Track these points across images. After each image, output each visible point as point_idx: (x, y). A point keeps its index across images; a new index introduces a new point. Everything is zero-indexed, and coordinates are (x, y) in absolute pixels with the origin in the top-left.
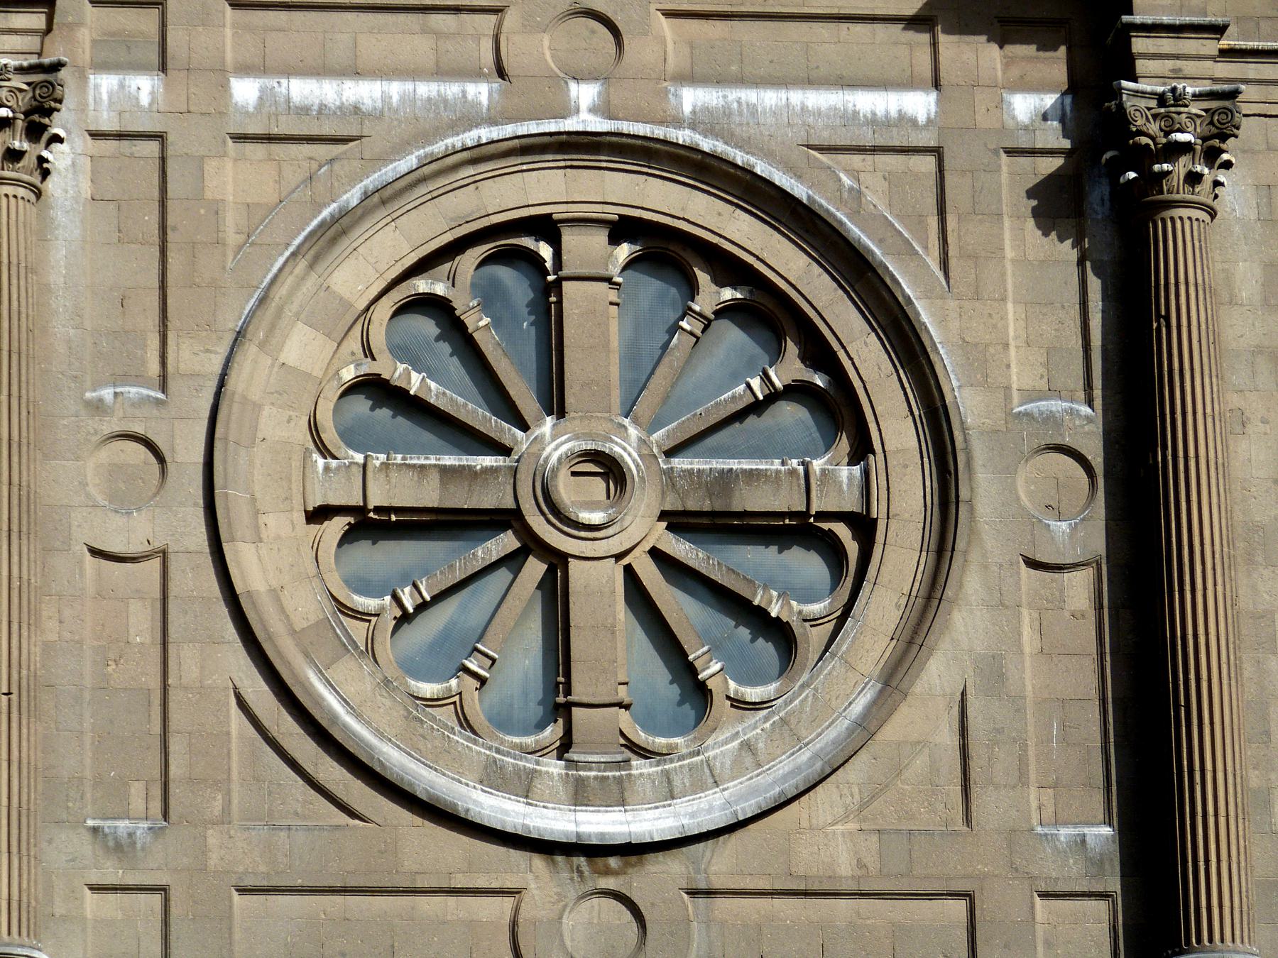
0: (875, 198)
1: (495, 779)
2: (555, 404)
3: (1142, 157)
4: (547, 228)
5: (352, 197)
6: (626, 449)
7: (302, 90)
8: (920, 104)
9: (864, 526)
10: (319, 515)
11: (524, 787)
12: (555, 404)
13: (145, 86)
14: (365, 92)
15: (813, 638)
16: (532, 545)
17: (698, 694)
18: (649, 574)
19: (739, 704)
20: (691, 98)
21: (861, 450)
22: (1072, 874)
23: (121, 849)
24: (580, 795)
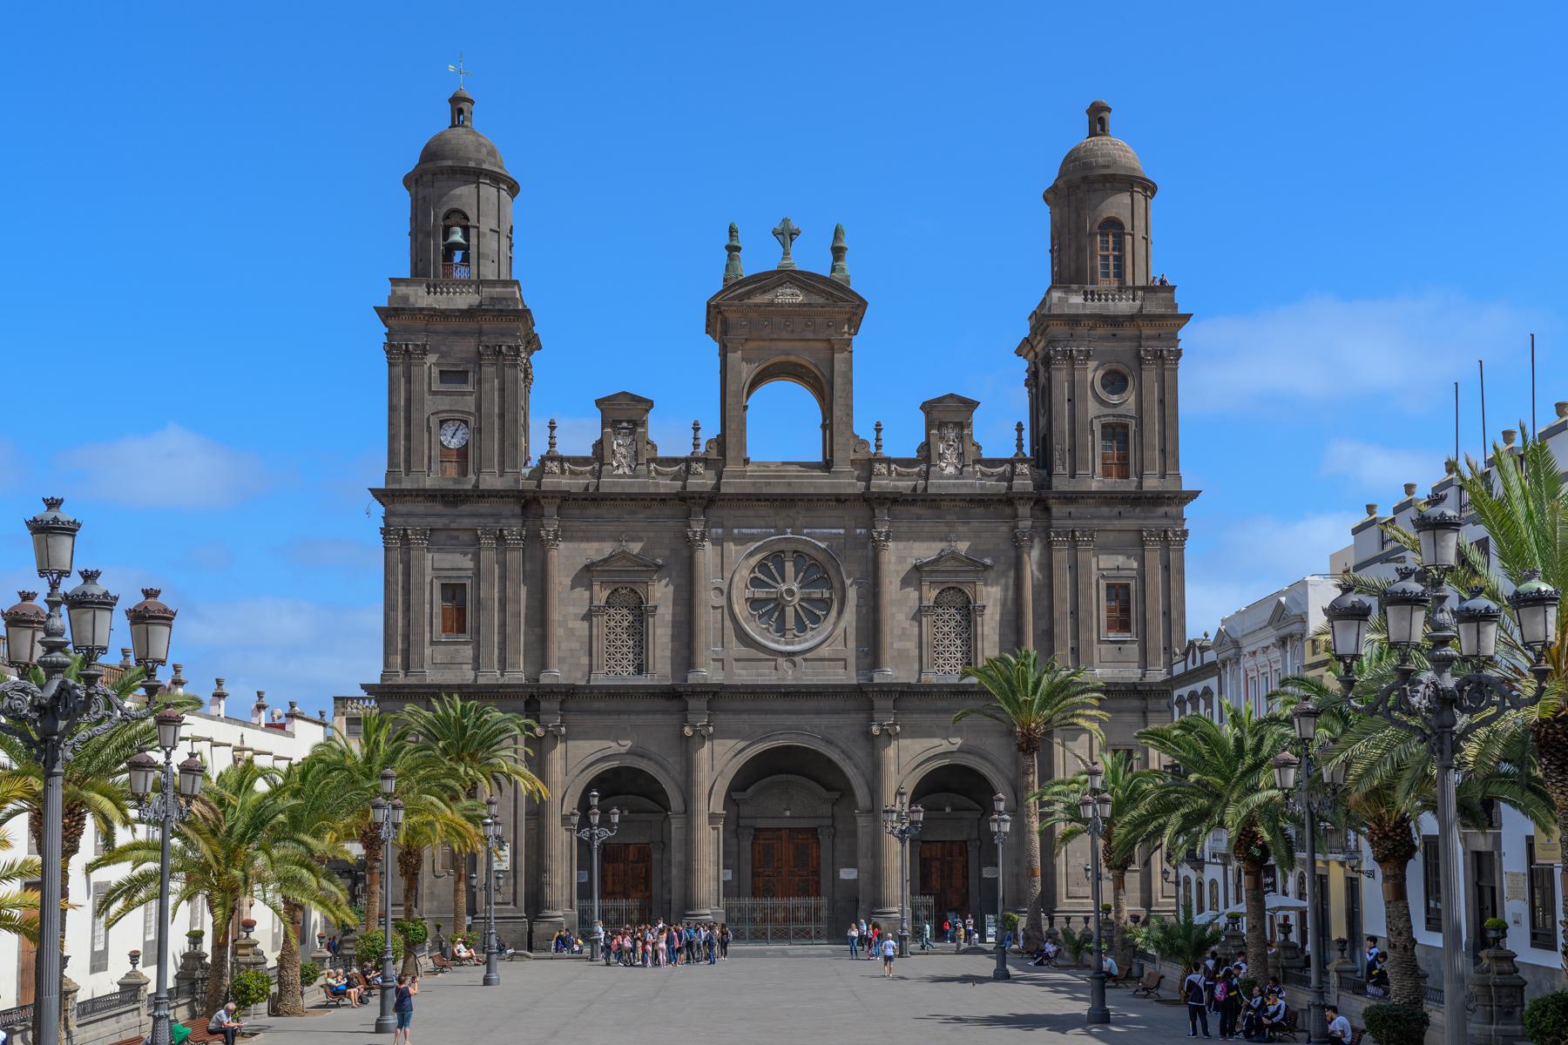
2: (784, 581)
3: (874, 541)
4: (783, 552)
6: (794, 588)
7: (744, 531)
8: (842, 531)
10: (747, 600)
11: (777, 642)
12: (784, 581)
13: (720, 531)
14: (754, 531)
15: (822, 618)
18: (797, 606)
20: (805, 531)
23: (717, 652)
24: (787, 644)
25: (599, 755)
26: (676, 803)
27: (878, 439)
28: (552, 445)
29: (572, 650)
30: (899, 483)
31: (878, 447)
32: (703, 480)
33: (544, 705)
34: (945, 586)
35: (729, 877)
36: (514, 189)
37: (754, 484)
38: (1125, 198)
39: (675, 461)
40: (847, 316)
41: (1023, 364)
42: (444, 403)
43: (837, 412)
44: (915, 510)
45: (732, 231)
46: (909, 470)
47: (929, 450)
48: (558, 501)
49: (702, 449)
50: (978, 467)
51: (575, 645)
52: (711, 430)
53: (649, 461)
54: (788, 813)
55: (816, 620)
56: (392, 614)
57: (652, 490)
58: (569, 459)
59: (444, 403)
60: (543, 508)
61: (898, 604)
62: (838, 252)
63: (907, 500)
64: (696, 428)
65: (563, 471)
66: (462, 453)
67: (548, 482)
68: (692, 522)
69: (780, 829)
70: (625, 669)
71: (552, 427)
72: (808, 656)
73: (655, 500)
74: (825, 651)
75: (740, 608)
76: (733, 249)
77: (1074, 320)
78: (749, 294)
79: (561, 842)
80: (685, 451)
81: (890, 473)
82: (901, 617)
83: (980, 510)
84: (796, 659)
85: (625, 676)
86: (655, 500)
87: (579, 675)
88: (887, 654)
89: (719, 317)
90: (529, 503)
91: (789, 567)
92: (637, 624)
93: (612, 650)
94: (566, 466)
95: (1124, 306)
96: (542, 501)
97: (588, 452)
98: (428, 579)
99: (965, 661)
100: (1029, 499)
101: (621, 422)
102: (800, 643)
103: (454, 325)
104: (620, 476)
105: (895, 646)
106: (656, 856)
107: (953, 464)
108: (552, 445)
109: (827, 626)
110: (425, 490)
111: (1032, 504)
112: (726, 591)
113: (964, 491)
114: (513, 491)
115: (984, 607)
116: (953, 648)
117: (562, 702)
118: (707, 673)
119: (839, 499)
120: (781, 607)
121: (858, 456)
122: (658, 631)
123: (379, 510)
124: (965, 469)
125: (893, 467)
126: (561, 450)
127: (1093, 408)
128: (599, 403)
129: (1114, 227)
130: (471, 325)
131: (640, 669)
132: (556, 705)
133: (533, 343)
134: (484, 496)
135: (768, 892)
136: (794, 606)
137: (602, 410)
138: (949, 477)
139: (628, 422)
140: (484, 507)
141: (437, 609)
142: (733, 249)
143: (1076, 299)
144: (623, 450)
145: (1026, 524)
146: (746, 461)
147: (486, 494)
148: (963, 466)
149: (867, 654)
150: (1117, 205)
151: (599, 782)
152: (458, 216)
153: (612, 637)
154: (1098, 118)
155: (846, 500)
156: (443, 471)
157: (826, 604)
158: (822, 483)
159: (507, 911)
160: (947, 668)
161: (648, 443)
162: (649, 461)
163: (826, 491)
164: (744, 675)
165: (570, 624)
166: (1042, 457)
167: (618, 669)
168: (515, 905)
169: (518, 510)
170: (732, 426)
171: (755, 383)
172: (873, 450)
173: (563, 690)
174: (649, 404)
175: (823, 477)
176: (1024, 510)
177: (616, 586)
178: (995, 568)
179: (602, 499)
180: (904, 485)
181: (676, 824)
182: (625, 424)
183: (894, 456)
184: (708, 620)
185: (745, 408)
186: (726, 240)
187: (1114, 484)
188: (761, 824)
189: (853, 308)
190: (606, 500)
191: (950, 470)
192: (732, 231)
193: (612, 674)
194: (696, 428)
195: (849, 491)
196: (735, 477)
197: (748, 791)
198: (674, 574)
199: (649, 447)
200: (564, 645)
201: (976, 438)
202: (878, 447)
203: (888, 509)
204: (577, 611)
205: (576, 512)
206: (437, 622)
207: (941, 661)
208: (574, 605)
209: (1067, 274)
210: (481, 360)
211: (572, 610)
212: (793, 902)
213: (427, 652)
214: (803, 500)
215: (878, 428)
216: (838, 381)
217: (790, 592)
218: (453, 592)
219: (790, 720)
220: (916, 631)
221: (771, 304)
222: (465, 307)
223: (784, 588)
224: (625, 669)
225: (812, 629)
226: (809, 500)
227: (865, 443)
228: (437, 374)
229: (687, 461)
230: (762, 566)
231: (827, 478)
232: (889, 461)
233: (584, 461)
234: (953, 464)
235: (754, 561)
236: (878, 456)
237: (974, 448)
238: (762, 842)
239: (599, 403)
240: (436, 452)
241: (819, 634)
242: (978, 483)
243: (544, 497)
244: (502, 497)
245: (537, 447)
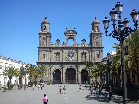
26: (61, 72)
32: (64, 46)
36: (49, 24)
38: (97, 24)
41: (90, 37)
52: (65, 42)
61: (80, 55)
67: (52, 47)
75: (67, 56)
77: (94, 34)
79: (52, 76)
85: (58, 62)
88: (78, 60)
90: (50, 48)
95: (98, 32)
97: (55, 44)
109: (74, 57)
118: (64, 62)
119: (75, 48)
123: (38, 49)
127: (95, 40)
129: (97, 26)
133: (51, 36)
143: (94, 32)
145: (90, 50)
150: (97, 25)
151: (54, 71)
152: (45, 26)
154: (95, 18)
166: (91, 44)
171: (68, 39)
180: (80, 47)
181: (61, 74)
184: (64, 57)
187: (97, 46)
189: (75, 33)
209: (93, 29)
212: (72, 80)
218: (44, 55)
219: (71, 66)
242: (86, 46)
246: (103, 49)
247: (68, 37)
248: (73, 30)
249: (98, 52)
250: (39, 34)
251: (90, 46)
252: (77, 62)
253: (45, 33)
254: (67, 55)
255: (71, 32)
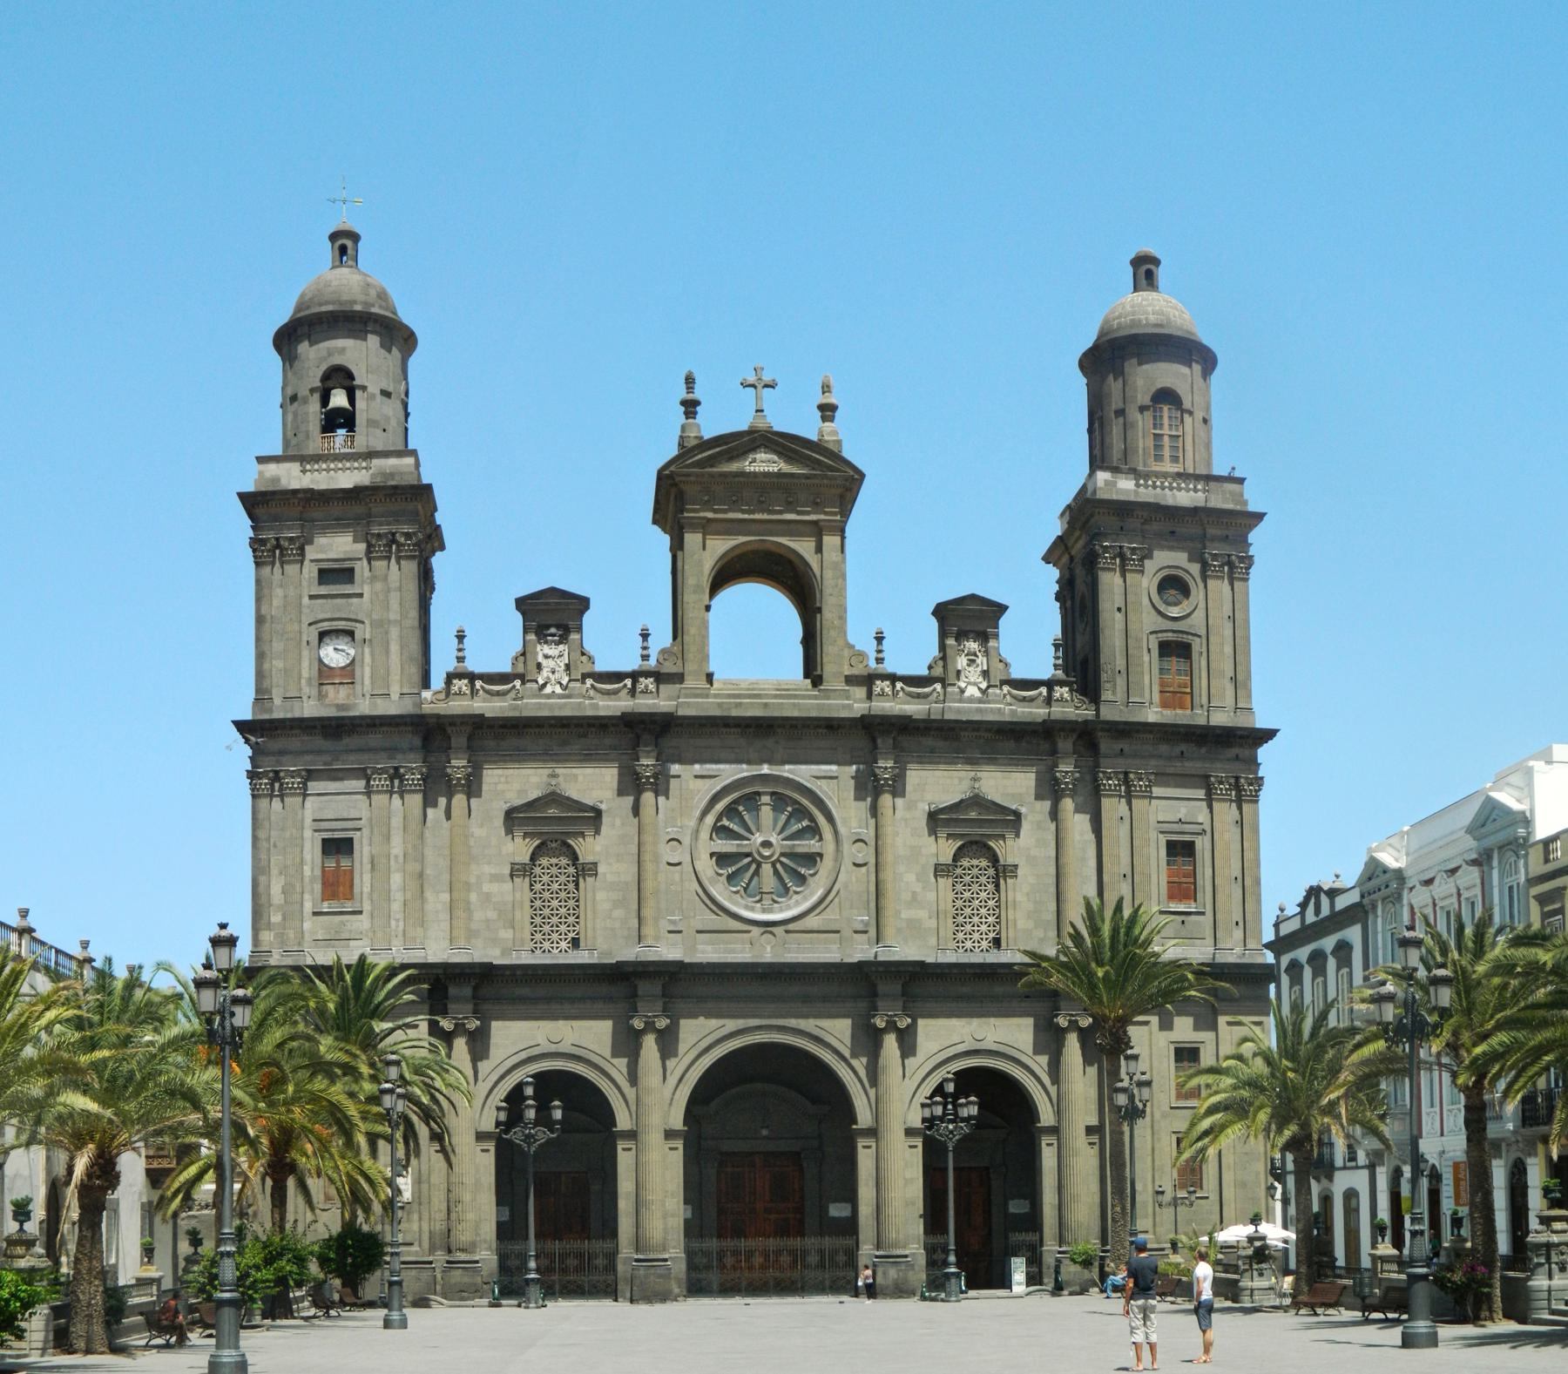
0: (825, 788)
1: (747, 908)
2: (758, 830)
4: (759, 794)
5: (718, 788)
6: (773, 840)
9: (821, 855)
10: (712, 855)
11: (752, 909)
16: (754, 860)
17: (787, 890)
18: (778, 866)
19: (796, 893)
21: (821, 839)
22: (860, 927)
23: (673, 922)
24: (764, 911)
25: (523, 1055)
27: (879, 651)
28: (460, 659)
29: (488, 920)
30: (906, 707)
31: (879, 661)
33: (452, 991)
34: (968, 839)
35: (689, 1215)
37: (720, 705)
39: (617, 677)
40: (839, 491)
42: (324, 609)
43: (828, 614)
44: (929, 742)
45: (690, 381)
46: (920, 690)
47: (945, 667)
48: (469, 729)
49: (652, 662)
50: (1006, 688)
51: (492, 915)
52: (662, 638)
53: (585, 676)
54: (765, 1132)
55: (802, 879)
56: (262, 879)
57: (590, 713)
58: (482, 677)
59: (324, 609)
60: (449, 738)
62: (827, 411)
63: (918, 729)
64: (645, 636)
65: (474, 692)
66: (349, 670)
67: (458, 706)
68: (641, 754)
69: (751, 1154)
70: (555, 945)
71: (461, 637)
72: (791, 927)
73: (593, 726)
74: (812, 922)
75: (706, 866)
76: (690, 407)
78: (712, 461)
80: (631, 663)
81: (895, 694)
82: (910, 877)
83: (1012, 744)
84: (778, 930)
85: (562, 955)
86: (593, 726)
87: (497, 952)
89: (673, 491)
91: (766, 812)
92: (571, 886)
93: (538, 920)
94: (478, 684)
96: (449, 730)
97: (507, 668)
98: (308, 833)
99: (992, 935)
100: (1073, 730)
101: (548, 627)
102: (781, 910)
103: (336, 509)
104: (548, 696)
105: (903, 916)
106: (595, 1187)
107: (975, 684)
108: (460, 659)
110: (302, 720)
111: (1075, 736)
112: (686, 840)
113: (990, 718)
114: (411, 716)
115: (1016, 866)
116: (976, 919)
117: (475, 988)
119: (830, 726)
120: (754, 866)
121: (855, 671)
122: (600, 896)
124: (990, 690)
125: (899, 685)
126: (472, 665)
128: (523, 604)
130: (358, 509)
131: (575, 943)
132: (467, 991)
134: (375, 725)
135: (739, 1233)
136: (773, 864)
137: (524, 614)
138: (971, 700)
139: (558, 627)
140: (374, 739)
141: (318, 872)
142: (690, 407)
144: (551, 663)
146: (710, 677)
147: (377, 722)
148: (988, 687)
149: (867, 924)
153: (538, 903)
155: (839, 727)
156: (321, 696)
157: (812, 859)
158: (812, 705)
159: (409, 1254)
160: (969, 944)
161: (583, 654)
162: (585, 676)
163: (814, 714)
164: (708, 952)
165: (486, 888)
167: (547, 945)
168: (420, 1246)
169: (418, 742)
170: (691, 631)
172: (873, 664)
173: (477, 971)
174: (582, 604)
175: (810, 697)
176: (1065, 745)
177: (545, 838)
178: (1029, 818)
179: (525, 726)
182: (553, 630)
183: (901, 672)
185: (708, 608)
186: (682, 393)
188: (727, 1146)
190: (530, 726)
191: (972, 691)
192: (690, 381)
193: (538, 952)
194: (645, 636)
195: (844, 714)
196: (696, 696)
197: (714, 1105)
198: (618, 822)
199: (584, 659)
200: (478, 915)
201: (1004, 653)
202: (879, 661)
203: (894, 739)
204: (493, 871)
205: (492, 743)
206: (318, 887)
207: (960, 936)
208: (489, 863)
210: (371, 552)
211: (488, 869)
212: (772, 1243)
213: (307, 925)
214: (784, 727)
215: (880, 639)
216: (828, 574)
217: (767, 844)
220: (931, 896)
221: (743, 474)
222: (350, 486)
223: (758, 838)
224: (555, 945)
225: (796, 893)
226: (791, 727)
227: (861, 655)
228: (315, 574)
229: (635, 676)
230: (730, 811)
231: (816, 697)
232: (893, 678)
233: (503, 678)
234: (975, 684)
235: (720, 806)
236: (880, 671)
237: (1001, 666)
238: (729, 1170)
239: (523, 604)
240: (315, 672)
241: (805, 899)
242: (1004, 707)
243: (452, 724)
244: (398, 725)
245: (442, 662)
246: (1264, 753)
247: (708, 552)
248: (808, 426)
249: (1182, 811)
250: (252, 502)
251: (1069, 707)
252: (861, 951)
253: (347, 478)
254: (708, 845)
255: (763, 463)
